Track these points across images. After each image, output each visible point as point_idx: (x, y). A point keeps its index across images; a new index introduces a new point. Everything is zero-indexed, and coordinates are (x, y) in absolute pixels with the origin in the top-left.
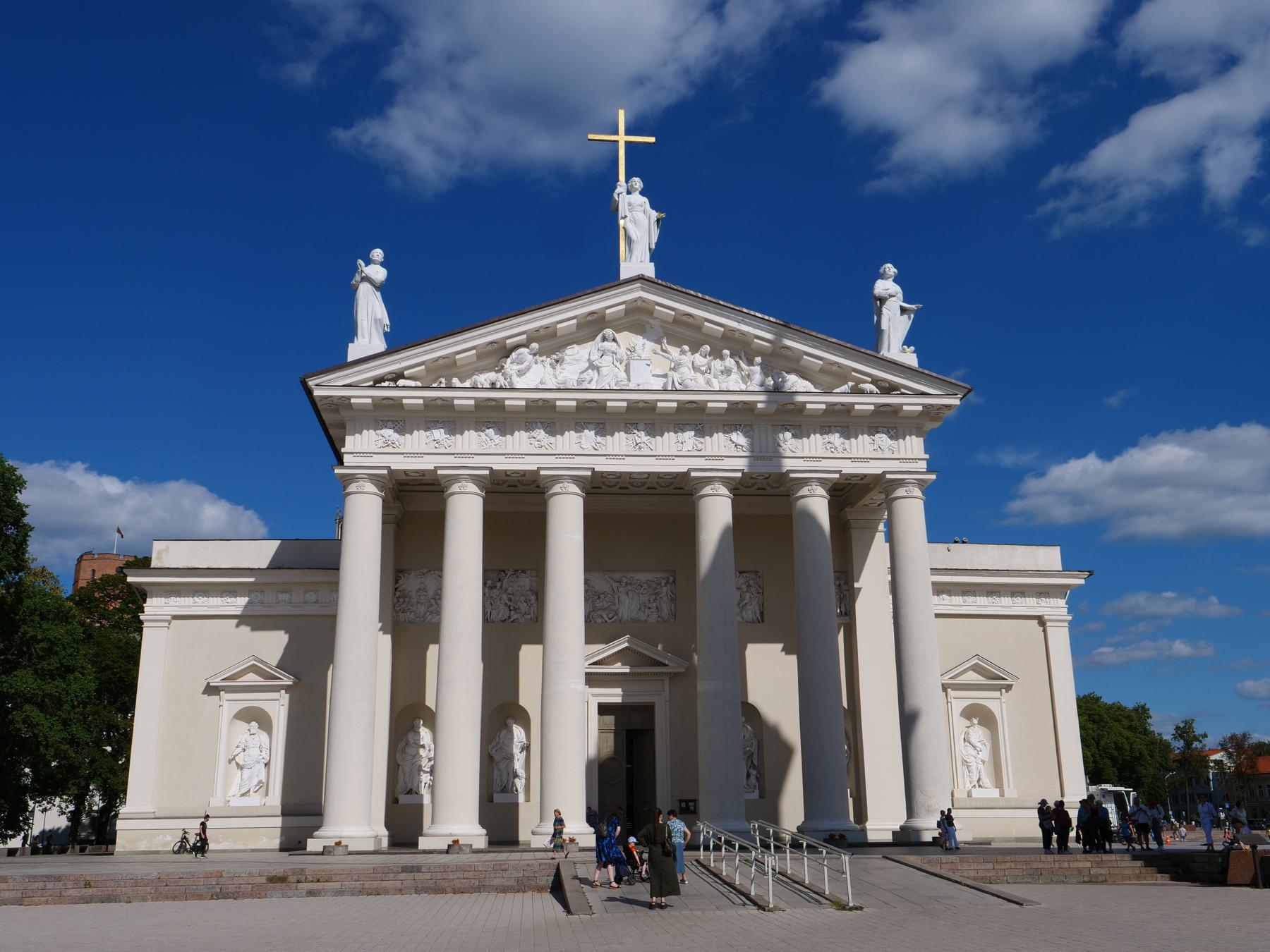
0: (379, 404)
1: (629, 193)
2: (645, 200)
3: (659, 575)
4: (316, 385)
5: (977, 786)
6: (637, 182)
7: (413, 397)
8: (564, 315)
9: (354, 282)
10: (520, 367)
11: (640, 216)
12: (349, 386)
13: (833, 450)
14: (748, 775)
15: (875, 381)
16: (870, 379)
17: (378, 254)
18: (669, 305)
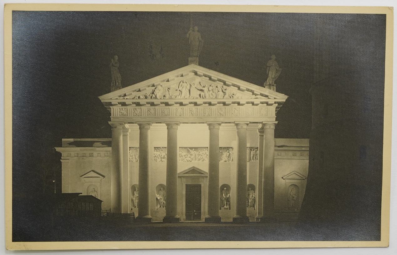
15: (262, 95)
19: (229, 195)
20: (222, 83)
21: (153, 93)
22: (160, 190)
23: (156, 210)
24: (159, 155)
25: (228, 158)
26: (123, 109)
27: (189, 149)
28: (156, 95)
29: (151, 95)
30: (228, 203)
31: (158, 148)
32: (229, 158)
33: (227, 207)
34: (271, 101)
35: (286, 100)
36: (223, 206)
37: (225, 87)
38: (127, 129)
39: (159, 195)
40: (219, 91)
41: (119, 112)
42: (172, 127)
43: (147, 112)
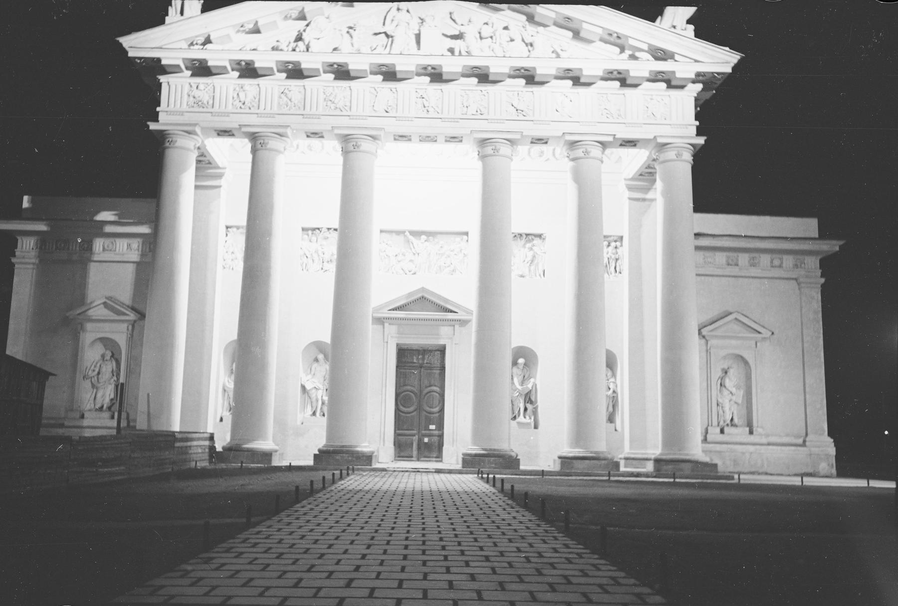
5: (730, 424)
13: (608, 116)
16: (645, 47)
19: (532, 380)
20: (524, 18)
21: (299, 38)
22: (316, 360)
23: (299, 423)
24: (316, 252)
25: (530, 265)
26: (201, 87)
27: (411, 237)
28: (309, 42)
29: (293, 45)
30: (529, 406)
31: (314, 229)
32: (532, 268)
33: (527, 420)
34: (684, 70)
35: (735, 68)
36: (514, 418)
37: (531, 29)
38: (218, 168)
39: (309, 377)
40: (512, 40)
41: (186, 96)
42: (356, 146)
43: (280, 97)
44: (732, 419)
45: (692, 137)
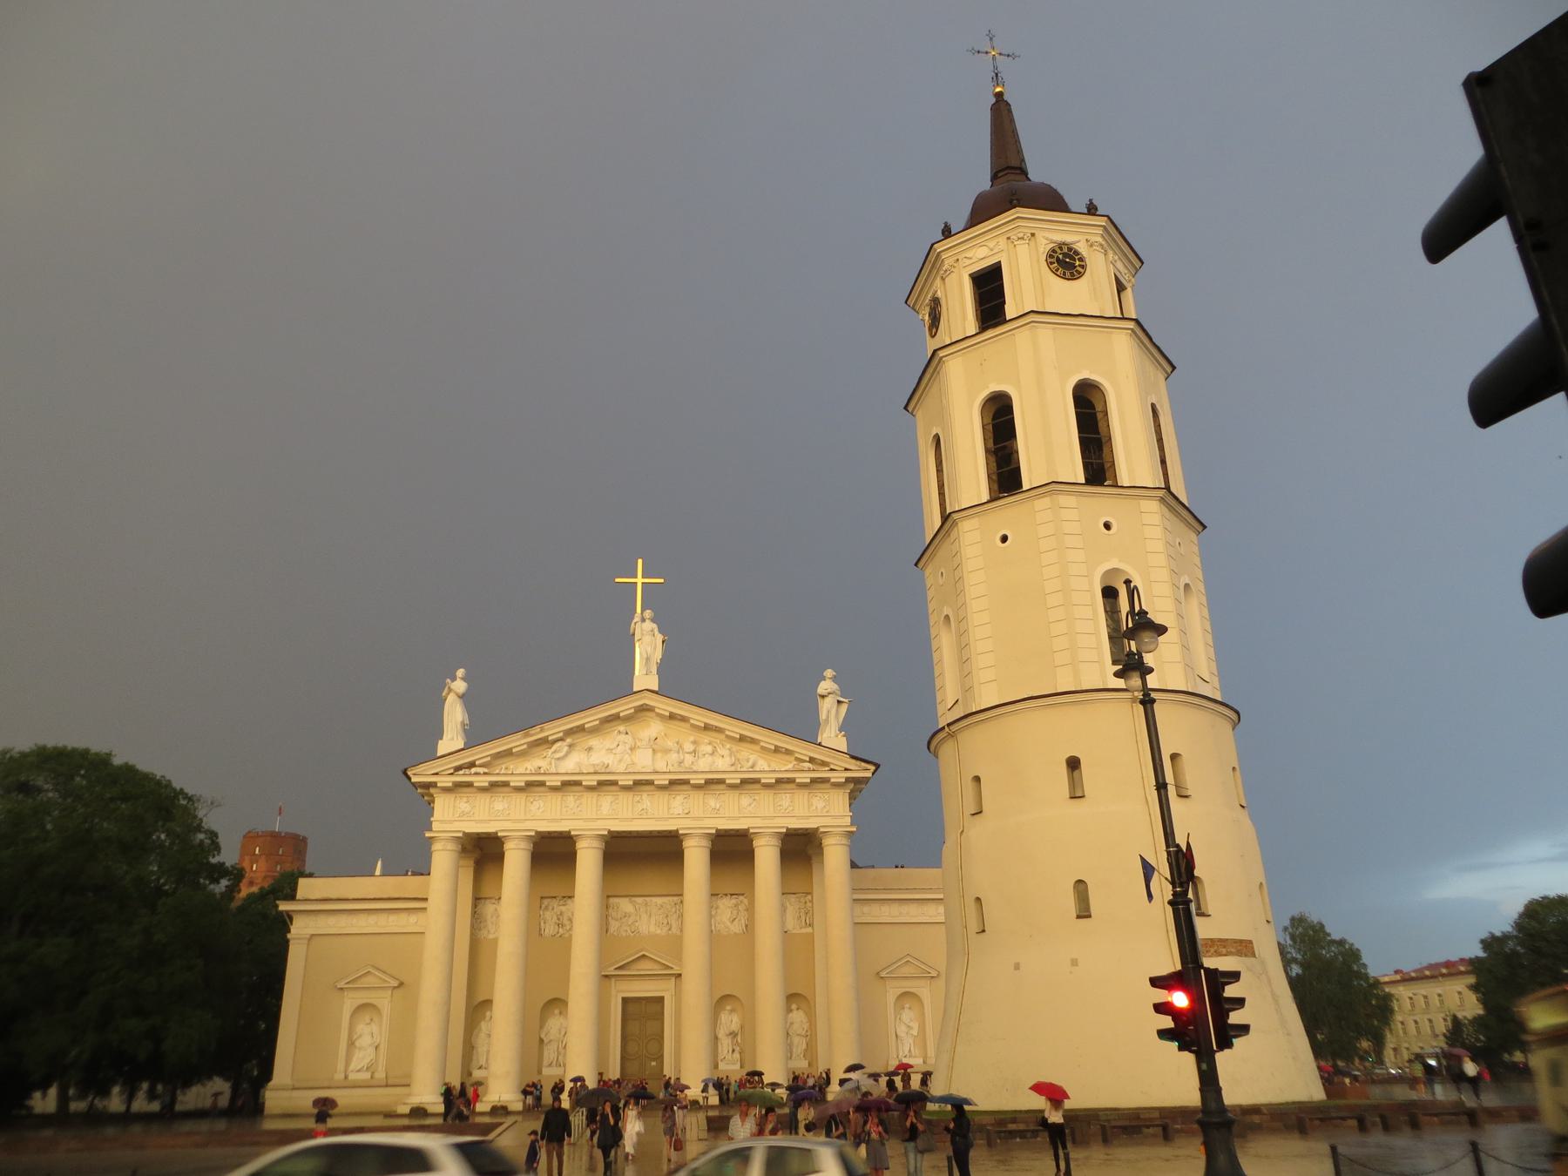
0: (458, 786)
1: (643, 620)
2: (655, 626)
3: (671, 898)
4: (414, 774)
6: (648, 613)
7: (481, 781)
8: (590, 718)
9: (444, 694)
10: (558, 755)
11: (647, 639)
12: (437, 774)
14: (733, 1051)
15: (812, 760)
16: (808, 759)
17: (460, 672)
18: (665, 706)
44: (910, 1051)
45: (847, 826)
